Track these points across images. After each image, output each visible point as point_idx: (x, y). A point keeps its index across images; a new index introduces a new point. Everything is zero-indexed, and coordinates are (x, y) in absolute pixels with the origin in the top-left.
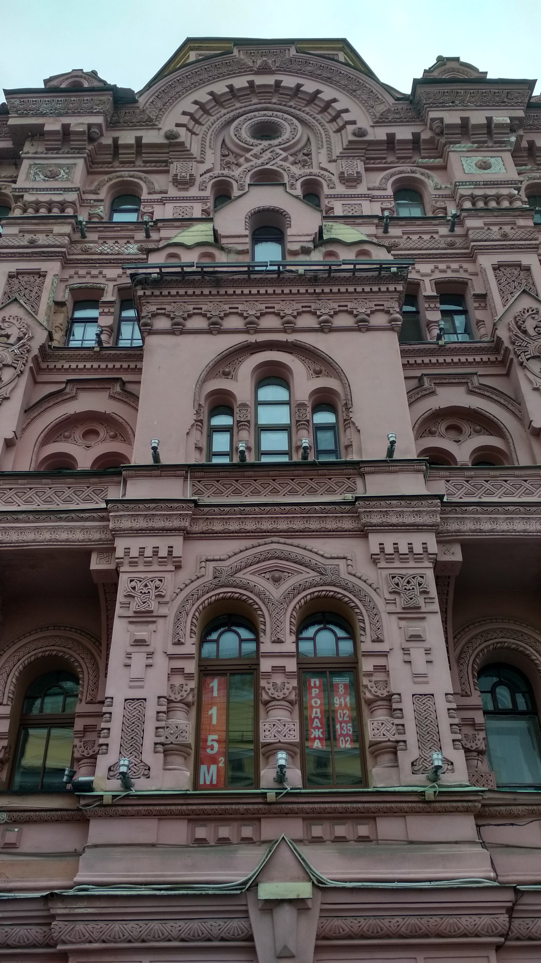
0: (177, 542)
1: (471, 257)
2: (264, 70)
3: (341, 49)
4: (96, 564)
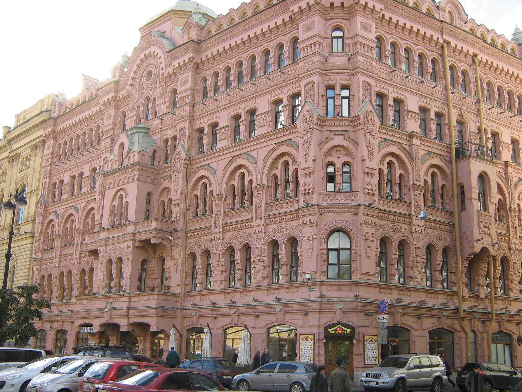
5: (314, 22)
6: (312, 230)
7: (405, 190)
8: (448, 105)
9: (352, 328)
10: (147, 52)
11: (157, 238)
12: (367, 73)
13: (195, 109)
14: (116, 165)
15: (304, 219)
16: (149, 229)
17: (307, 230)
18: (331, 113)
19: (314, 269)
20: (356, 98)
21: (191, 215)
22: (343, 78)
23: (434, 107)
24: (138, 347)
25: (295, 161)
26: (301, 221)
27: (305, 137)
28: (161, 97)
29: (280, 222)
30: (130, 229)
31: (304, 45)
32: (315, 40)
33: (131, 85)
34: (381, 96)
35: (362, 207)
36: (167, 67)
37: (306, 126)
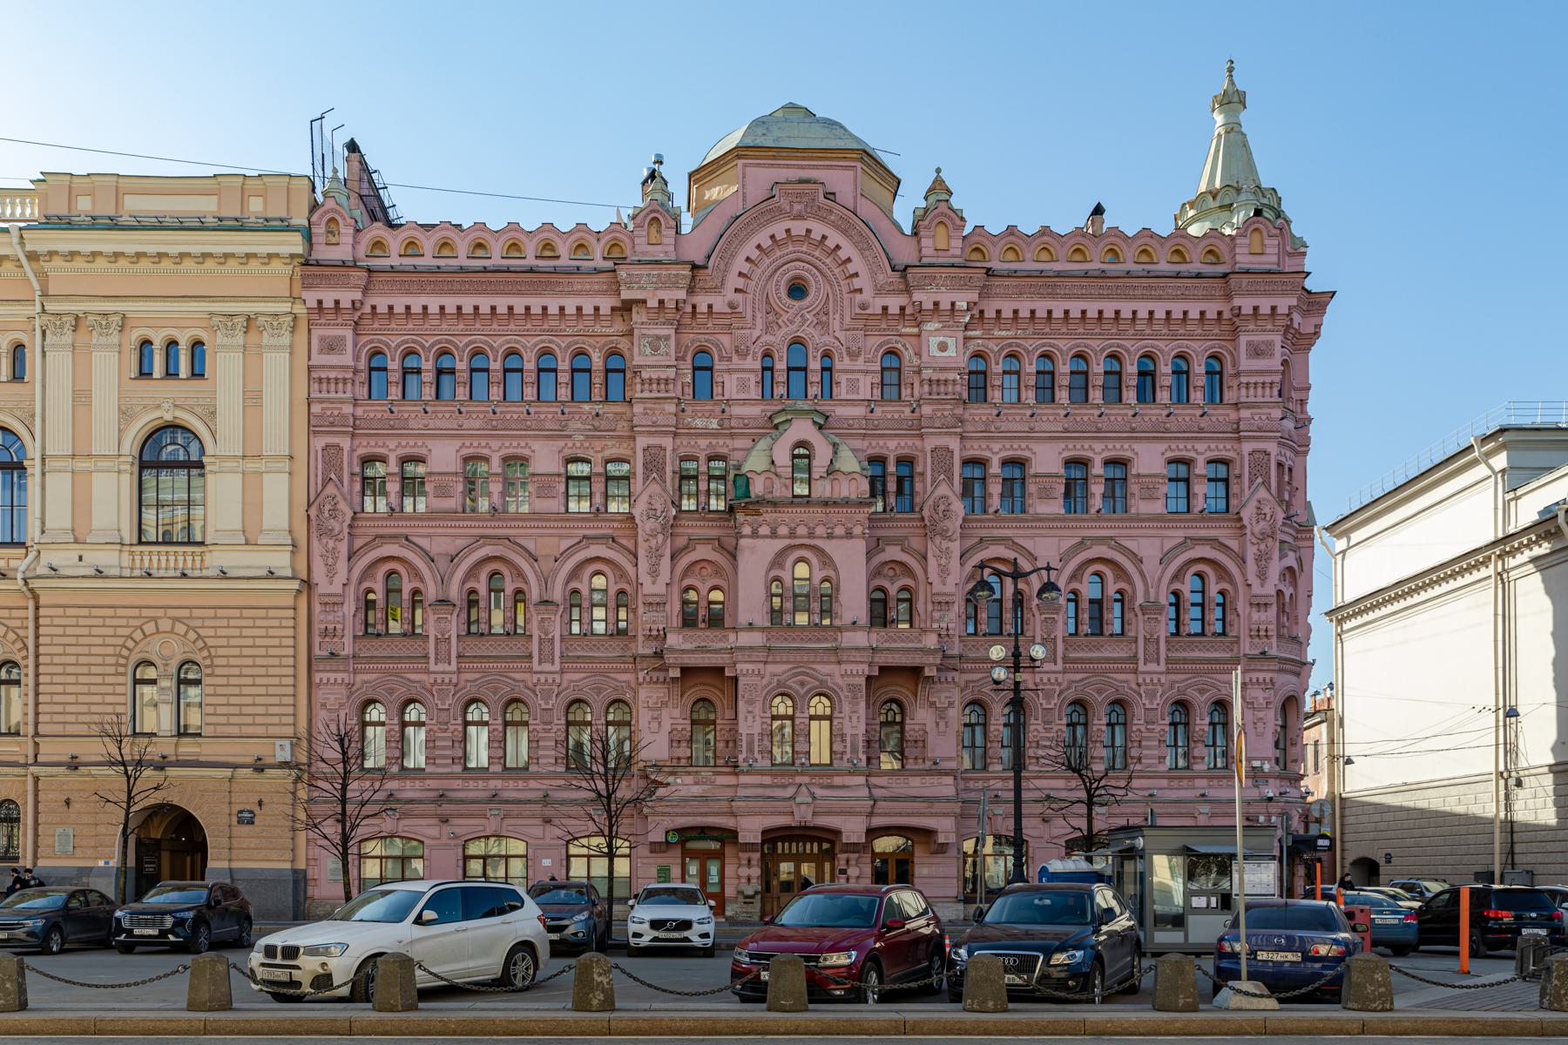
0: (761, 666)
1: (921, 436)
4: (727, 673)
27: (1263, 547)
28: (853, 355)
29: (1197, 673)
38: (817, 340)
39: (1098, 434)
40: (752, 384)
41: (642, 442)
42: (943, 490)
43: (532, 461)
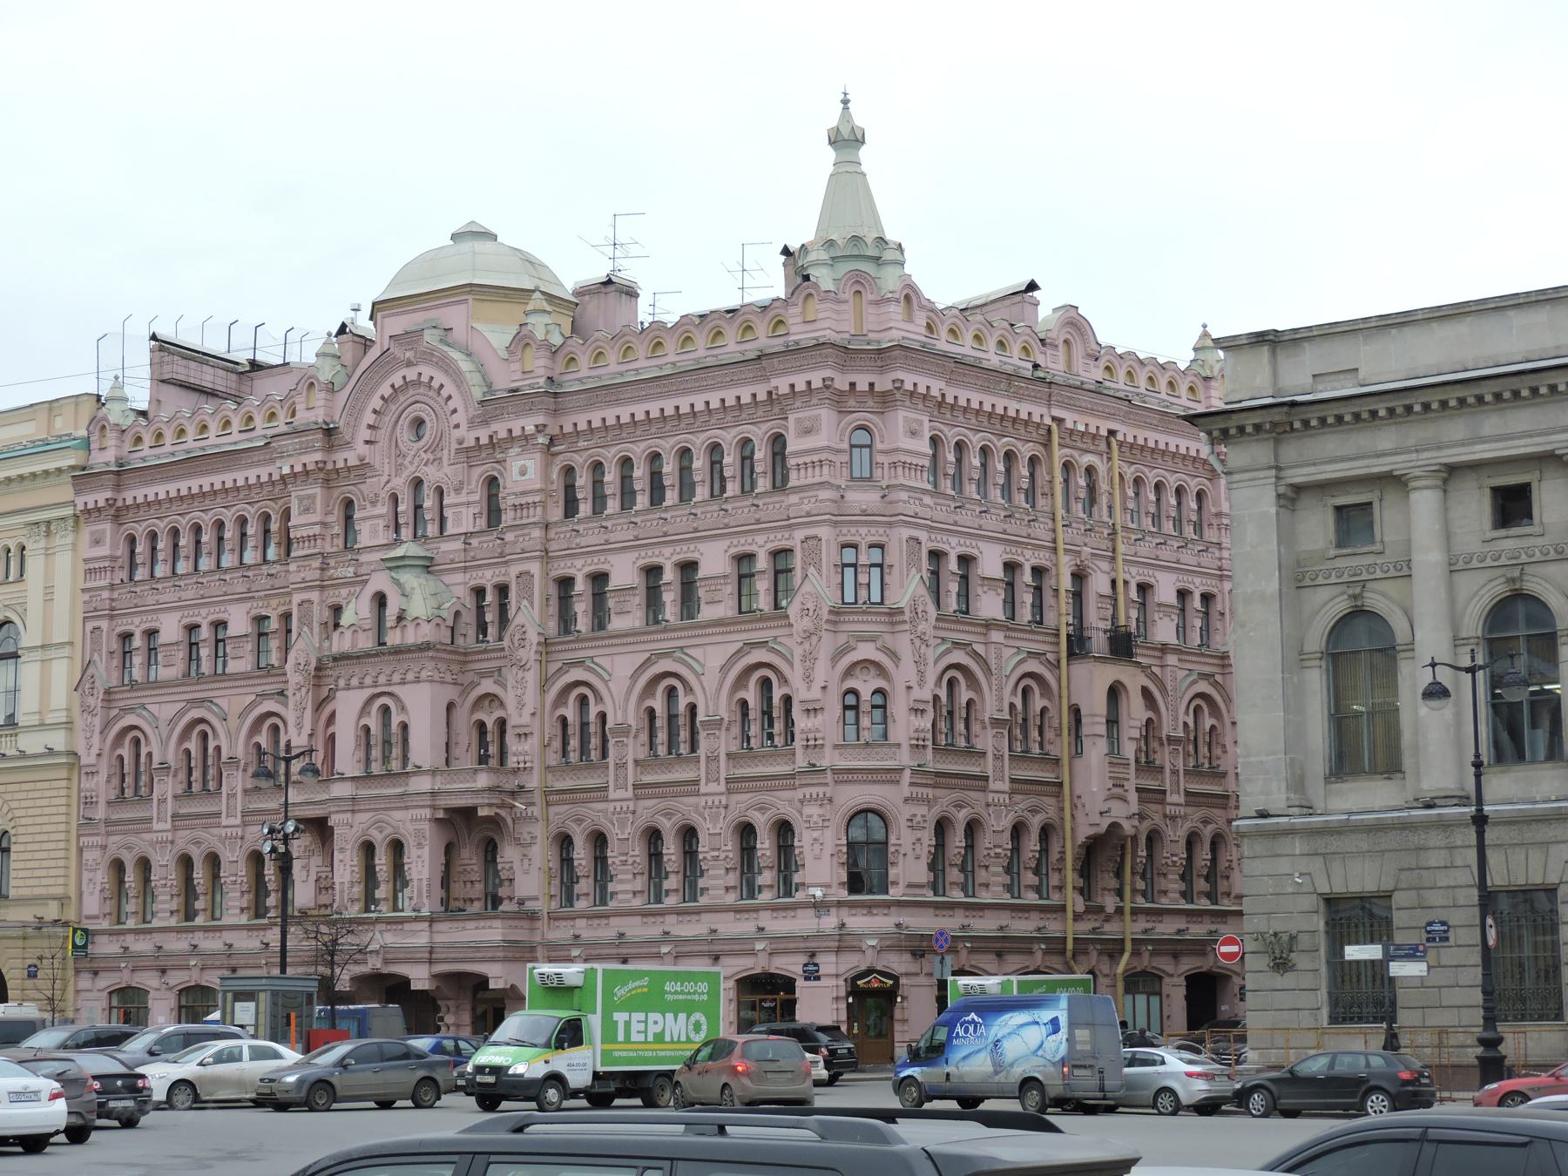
0: (349, 815)
2: (409, 364)
3: (469, 293)
5: (818, 418)
6: (820, 811)
7: (976, 728)
8: (1055, 549)
9: (896, 978)
10: (411, 374)
11: (490, 805)
12: (914, 521)
13: (552, 534)
14: (366, 642)
15: (808, 791)
16: (472, 786)
17: (813, 810)
18: (849, 598)
19: (827, 880)
20: (896, 570)
21: (553, 759)
22: (873, 530)
23: (1029, 559)
24: (442, 1019)
25: (784, 680)
26: (799, 794)
28: (458, 490)
30: (422, 784)
31: (801, 461)
32: (823, 456)
33: (367, 442)
34: (936, 556)
35: (907, 773)
36: (472, 424)
37: (807, 623)
38: (431, 475)
39: (666, 540)
40: (381, 528)
41: (297, 598)
42: (519, 620)
43: (230, 625)
